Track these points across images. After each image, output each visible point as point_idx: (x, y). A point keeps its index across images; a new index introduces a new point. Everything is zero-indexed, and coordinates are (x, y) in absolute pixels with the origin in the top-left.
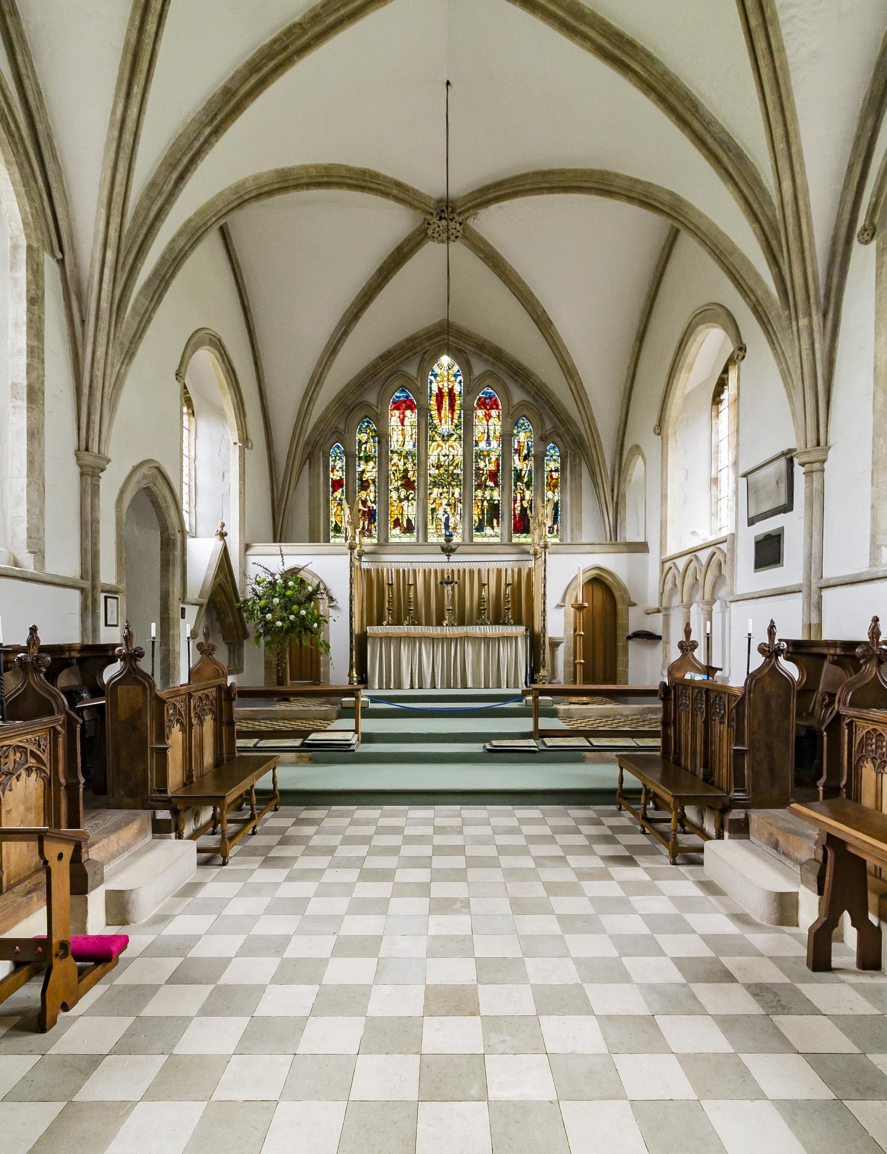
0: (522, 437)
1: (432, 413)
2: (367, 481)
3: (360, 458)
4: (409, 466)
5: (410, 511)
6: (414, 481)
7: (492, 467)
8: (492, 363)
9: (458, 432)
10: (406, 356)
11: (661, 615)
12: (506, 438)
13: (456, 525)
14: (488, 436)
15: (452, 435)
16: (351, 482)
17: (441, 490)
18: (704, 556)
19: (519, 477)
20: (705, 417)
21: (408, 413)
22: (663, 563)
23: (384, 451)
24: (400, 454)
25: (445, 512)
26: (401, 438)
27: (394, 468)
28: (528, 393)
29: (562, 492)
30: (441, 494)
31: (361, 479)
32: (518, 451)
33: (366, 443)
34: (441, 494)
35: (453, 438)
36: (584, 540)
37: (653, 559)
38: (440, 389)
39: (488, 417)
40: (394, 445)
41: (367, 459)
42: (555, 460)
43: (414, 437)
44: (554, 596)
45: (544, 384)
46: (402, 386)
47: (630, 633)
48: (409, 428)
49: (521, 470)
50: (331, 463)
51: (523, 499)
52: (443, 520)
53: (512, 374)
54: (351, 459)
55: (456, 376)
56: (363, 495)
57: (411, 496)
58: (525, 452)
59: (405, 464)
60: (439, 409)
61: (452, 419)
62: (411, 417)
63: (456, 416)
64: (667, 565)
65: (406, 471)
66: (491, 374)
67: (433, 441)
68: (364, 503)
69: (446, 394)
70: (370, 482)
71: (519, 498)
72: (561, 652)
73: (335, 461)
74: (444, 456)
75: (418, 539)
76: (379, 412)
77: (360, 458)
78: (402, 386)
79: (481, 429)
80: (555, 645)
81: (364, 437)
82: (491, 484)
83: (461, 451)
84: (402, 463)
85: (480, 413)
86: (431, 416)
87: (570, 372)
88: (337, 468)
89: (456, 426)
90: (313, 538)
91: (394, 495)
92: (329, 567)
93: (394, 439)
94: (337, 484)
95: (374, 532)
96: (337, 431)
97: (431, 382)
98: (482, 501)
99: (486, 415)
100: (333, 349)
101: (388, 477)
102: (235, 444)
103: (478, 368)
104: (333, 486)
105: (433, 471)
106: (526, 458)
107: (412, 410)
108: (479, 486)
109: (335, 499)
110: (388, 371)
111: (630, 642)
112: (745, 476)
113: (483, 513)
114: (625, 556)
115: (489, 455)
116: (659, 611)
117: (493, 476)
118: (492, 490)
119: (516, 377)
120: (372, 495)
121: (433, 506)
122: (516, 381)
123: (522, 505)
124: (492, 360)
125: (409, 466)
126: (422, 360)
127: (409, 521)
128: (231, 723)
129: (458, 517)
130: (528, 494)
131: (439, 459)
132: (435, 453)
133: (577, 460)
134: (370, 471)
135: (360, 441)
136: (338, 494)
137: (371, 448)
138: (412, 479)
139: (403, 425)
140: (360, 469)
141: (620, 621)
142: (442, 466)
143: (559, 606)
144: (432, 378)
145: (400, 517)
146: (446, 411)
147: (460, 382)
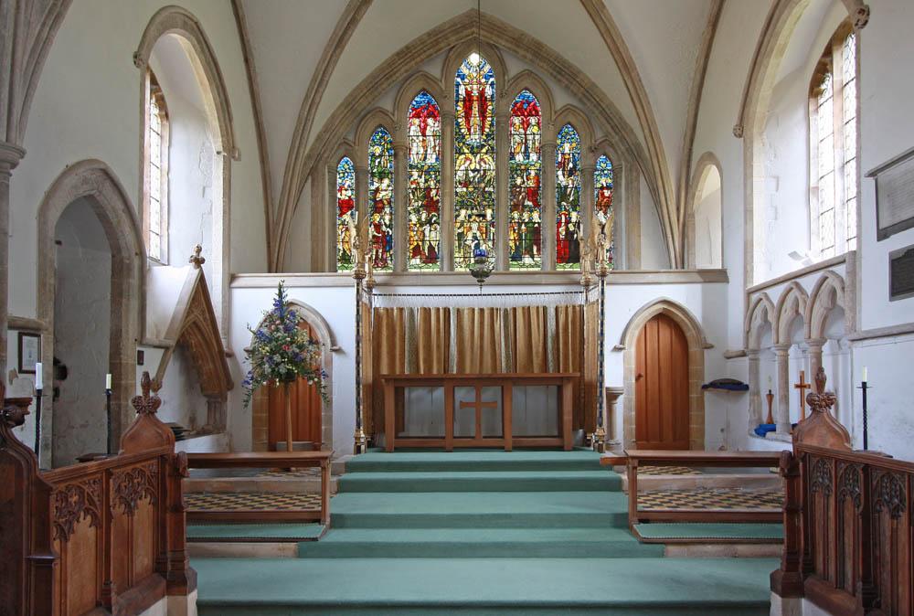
0: (567, 147)
1: (460, 120)
3: (373, 175)
4: (432, 184)
5: (432, 235)
7: (531, 184)
8: (531, 60)
9: (490, 142)
10: (428, 53)
11: (746, 359)
14: (527, 148)
15: (483, 146)
16: (362, 202)
17: (469, 212)
18: (809, 283)
20: (800, 113)
21: (430, 121)
22: (749, 293)
23: (400, 165)
24: (420, 170)
25: (475, 238)
26: (422, 151)
27: (414, 186)
30: (470, 216)
31: (374, 200)
32: (562, 165)
33: (380, 156)
34: (470, 216)
35: (484, 150)
36: (643, 268)
37: (735, 293)
38: (468, 93)
39: (526, 125)
40: (414, 159)
41: (382, 176)
43: (437, 148)
44: (611, 340)
45: (594, 84)
46: (424, 90)
47: (707, 382)
48: (432, 139)
50: (339, 181)
51: (568, 222)
53: (555, 73)
54: (361, 174)
55: (487, 77)
56: (377, 218)
57: (434, 219)
59: (426, 181)
60: (468, 116)
61: (482, 129)
63: (487, 124)
64: (755, 297)
65: (428, 189)
67: (461, 154)
68: (378, 227)
69: (475, 98)
71: (563, 220)
72: (619, 405)
74: (473, 171)
75: (442, 269)
76: (395, 119)
77: (373, 175)
78: (424, 90)
80: (613, 396)
81: (378, 150)
82: (530, 204)
83: (493, 166)
84: (423, 180)
85: (517, 120)
86: (458, 124)
87: (625, 66)
88: (346, 186)
89: (488, 135)
90: (316, 268)
91: (414, 218)
92: (331, 303)
93: (414, 150)
94: (346, 206)
95: (389, 262)
97: (458, 85)
98: (520, 225)
99: (522, 124)
100: (339, 41)
101: (407, 196)
102: (218, 153)
103: (514, 67)
104: (341, 208)
106: (571, 173)
108: (515, 207)
110: (406, 71)
111: (707, 394)
112: (873, 174)
114: (699, 287)
115: (527, 170)
116: (743, 354)
117: (533, 194)
118: (532, 211)
119: (559, 77)
120: (387, 218)
121: (460, 231)
122: (560, 81)
123: (567, 229)
124: (529, 56)
125: (432, 184)
127: (431, 248)
128: (178, 508)
129: (490, 243)
130: (574, 216)
131: (467, 175)
132: (462, 168)
133: (635, 174)
134: (385, 189)
135: (373, 155)
136: (347, 217)
137: (389, 165)
138: (435, 199)
139: (424, 135)
140: (373, 188)
141: (693, 368)
142: (470, 183)
143: (617, 349)
144: (459, 80)
145: (420, 243)
146: (475, 120)
147: (492, 84)
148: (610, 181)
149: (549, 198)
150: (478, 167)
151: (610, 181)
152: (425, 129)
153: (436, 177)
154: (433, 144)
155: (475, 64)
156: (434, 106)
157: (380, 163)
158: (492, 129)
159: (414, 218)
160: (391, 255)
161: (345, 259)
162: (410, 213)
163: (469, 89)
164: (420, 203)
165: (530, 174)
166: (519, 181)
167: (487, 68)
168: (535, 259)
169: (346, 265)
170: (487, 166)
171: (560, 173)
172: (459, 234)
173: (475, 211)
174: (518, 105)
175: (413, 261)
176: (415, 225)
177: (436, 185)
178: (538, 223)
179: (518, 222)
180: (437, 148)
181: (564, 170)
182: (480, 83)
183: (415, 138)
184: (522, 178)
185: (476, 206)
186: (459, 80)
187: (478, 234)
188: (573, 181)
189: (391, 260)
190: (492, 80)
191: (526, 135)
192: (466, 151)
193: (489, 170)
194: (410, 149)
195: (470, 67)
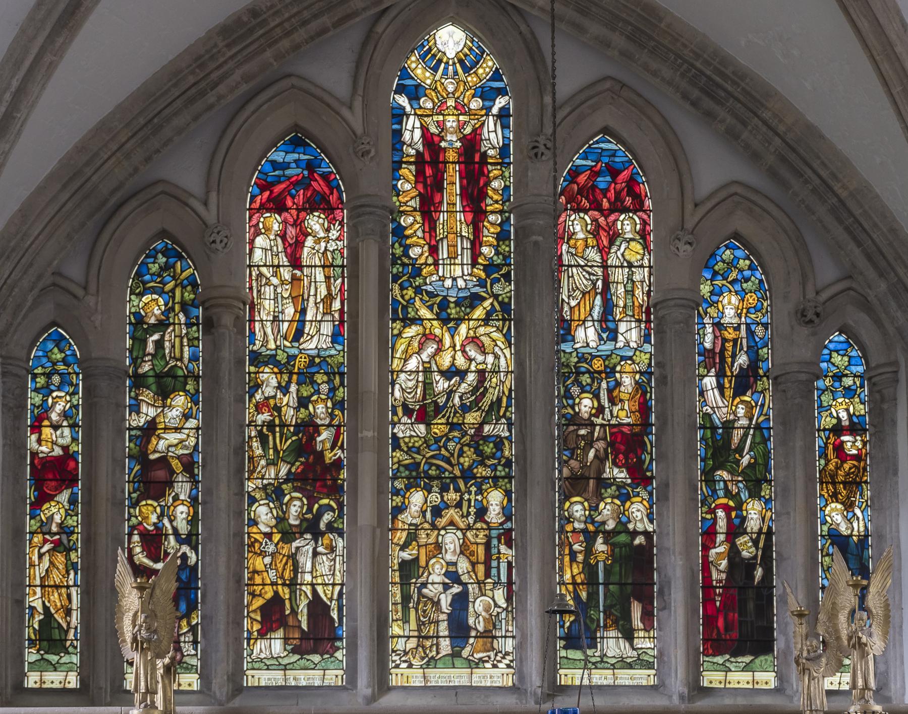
0: (729, 307)
2: (164, 461)
3: (139, 381)
5: (323, 570)
6: (338, 464)
8: (623, 53)
9: (497, 288)
10: (314, 26)
12: (670, 315)
13: (493, 622)
14: (608, 307)
15: (474, 300)
16: (104, 466)
17: (435, 498)
19: (721, 450)
21: (315, 222)
23: (226, 354)
24: (284, 367)
25: (453, 577)
27: (261, 418)
28: (755, 157)
29: (875, 504)
31: (141, 457)
32: (716, 359)
33: (162, 325)
34: (437, 512)
35: (479, 313)
40: (266, 336)
41: (166, 385)
42: (849, 392)
43: (337, 305)
45: (810, 128)
46: (296, 128)
48: (320, 276)
49: (728, 426)
51: (735, 530)
52: (445, 601)
53: (695, 93)
54: (103, 389)
56: (149, 513)
57: (327, 517)
58: (742, 360)
59: (303, 402)
60: (428, 209)
61: (476, 244)
62: (324, 236)
63: (489, 234)
65: (309, 427)
66: (616, 89)
67: (409, 322)
69: (451, 156)
70: (176, 464)
71: (722, 525)
73: (46, 390)
75: (351, 672)
76: (211, 217)
77: (139, 381)
78: (296, 128)
79: (580, 279)
81: (153, 306)
82: (621, 475)
83: (506, 359)
84: (290, 399)
85: (578, 225)
86: (399, 232)
88: (54, 417)
89: (490, 268)
91: (264, 513)
94: (54, 474)
95: (188, 649)
96: (57, 284)
97: (399, 115)
98: (590, 538)
101: (241, 448)
103: (574, 70)
104: (38, 479)
105: (408, 430)
106: (744, 383)
107: (329, 210)
108: (575, 484)
109: (44, 529)
110: (247, 78)
113: (591, 580)
115: (610, 371)
117: (627, 445)
118: (625, 498)
119: (707, 103)
120: (182, 511)
121: (406, 555)
122: (709, 115)
123: (733, 554)
124: (619, 41)
126: (369, 39)
127: (317, 607)
129: (500, 596)
130: (754, 511)
131: (428, 385)
134: (176, 426)
135: (139, 320)
136: (55, 511)
137: (180, 345)
138: (329, 457)
139: (296, 263)
142: (438, 410)
144: (403, 101)
145: (285, 593)
146: (453, 218)
147: (503, 115)
148: (861, 409)
149: (677, 459)
150: (461, 361)
151: (861, 409)
152: (299, 244)
153: (333, 390)
154: (323, 291)
155: (451, 54)
156: (326, 177)
157: (159, 344)
158: (504, 248)
159: (264, 513)
160: (193, 629)
161: (50, 640)
162: (253, 500)
163: (433, 130)
164: (284, 470)
165: (618, 384)
166: (586, 404)
167: (488, 65)
168: (638, 643)
169: (54, 658)
170: (490, 359)
171: (710, 382)
172: (404, 564)
173: (452, 496)
174: (582, 179)
175: (260, 648)
176: (269, 536)
177: (332, 416)
178: (646, 533)
179: (585, 531)
180: (337, 305)
181: (720, 375)
182: (461, 108)
183: (264, 270)
184: (596, 396)
185: (454, 479)
186: (403, 101)
187: (463, 566)
188: (749, 407)
189: (195, 642)
190: (500, 102)
191: (605, 266)
192: (425, 313)
193: (496, 372)
194: (252, 306)
195: (434, 61)
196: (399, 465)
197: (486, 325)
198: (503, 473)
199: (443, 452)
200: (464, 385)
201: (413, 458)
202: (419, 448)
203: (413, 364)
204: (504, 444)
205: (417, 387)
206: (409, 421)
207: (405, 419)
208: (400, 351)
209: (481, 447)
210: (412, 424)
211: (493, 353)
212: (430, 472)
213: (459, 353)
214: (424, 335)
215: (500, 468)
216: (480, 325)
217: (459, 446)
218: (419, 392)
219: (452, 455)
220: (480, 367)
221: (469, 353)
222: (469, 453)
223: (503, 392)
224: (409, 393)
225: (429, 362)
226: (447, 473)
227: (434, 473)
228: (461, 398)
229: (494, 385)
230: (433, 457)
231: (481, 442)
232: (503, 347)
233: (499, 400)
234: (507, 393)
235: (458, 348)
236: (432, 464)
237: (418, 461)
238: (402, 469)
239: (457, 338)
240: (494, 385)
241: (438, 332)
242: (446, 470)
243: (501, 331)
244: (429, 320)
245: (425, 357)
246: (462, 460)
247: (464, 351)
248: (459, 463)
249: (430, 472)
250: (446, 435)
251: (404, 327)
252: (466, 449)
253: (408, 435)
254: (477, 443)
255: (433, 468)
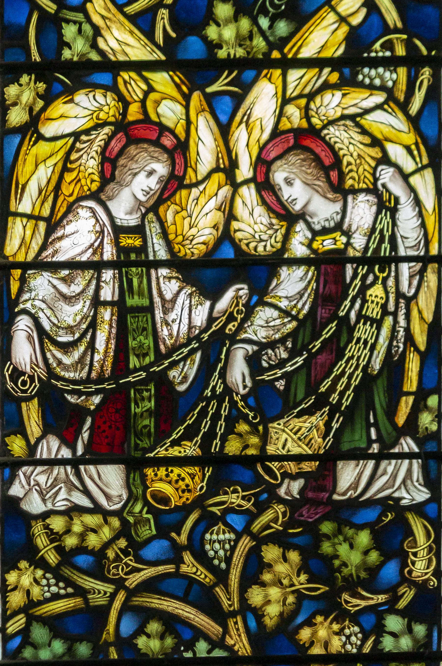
74: (206, 272)
150: (254, 224)
170: (362, 212)
196: (31, 619)
197: (349, 82)
198: (405, 643)
199: (190, 566)
200: (264, 314)
201: (81, 592)
202: (100, 554)
203: (79, 237)
204: (410, 533)
205: (93, 325)
206: (66, 453)
207: (51, 447)
208: (32, 189)
209: (326, 548)
210: (75, 463)
211: (373, 190)
212: (141, 642)
213: (249, 193)
214: (121, 126)
215: (394, 623)
216: (326, 86)
217: (246, 543)
218: (100, 344)
219: (222, 577)
220: (326, 244)
221: (286, 193)
222: (281, 568)
223: (409, 338)
224: (66, 347)
225: (139, 230)
226: (202, 647)
227: (155, 645)
228: (253, 361)
229: (374, 311)
230: (150, 586)
231: (327, 527)
232: (409, 165)
233: (394, 367)
234: (421, 340)
235: (245, 171)
236: (147, 614)
237: (98, 600)
238: (39, 633)
239: (240, 136)
240: (374, 311)
241: (170, 112)
242: (199, 634)
243: (404, 107)
244: (139, 67)
245: (123, 208)
246: (256, 596)
247: (264, 185)
248: (246, 608)
249: (141, 642)
250: (199, 502)
251: (48, 98)
252: (271, 553)
253: (61, 505)
254: (312, 530)
255: (154, 627)
